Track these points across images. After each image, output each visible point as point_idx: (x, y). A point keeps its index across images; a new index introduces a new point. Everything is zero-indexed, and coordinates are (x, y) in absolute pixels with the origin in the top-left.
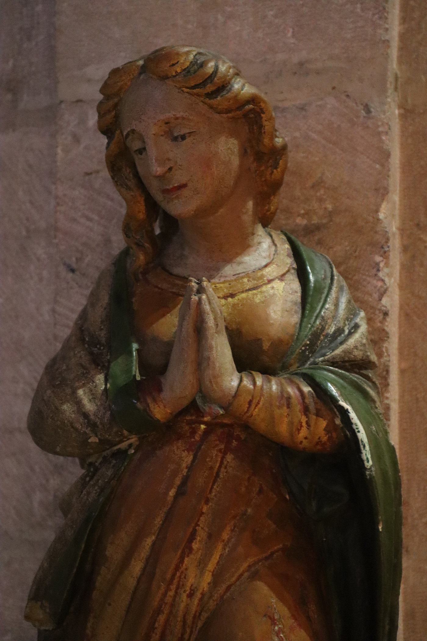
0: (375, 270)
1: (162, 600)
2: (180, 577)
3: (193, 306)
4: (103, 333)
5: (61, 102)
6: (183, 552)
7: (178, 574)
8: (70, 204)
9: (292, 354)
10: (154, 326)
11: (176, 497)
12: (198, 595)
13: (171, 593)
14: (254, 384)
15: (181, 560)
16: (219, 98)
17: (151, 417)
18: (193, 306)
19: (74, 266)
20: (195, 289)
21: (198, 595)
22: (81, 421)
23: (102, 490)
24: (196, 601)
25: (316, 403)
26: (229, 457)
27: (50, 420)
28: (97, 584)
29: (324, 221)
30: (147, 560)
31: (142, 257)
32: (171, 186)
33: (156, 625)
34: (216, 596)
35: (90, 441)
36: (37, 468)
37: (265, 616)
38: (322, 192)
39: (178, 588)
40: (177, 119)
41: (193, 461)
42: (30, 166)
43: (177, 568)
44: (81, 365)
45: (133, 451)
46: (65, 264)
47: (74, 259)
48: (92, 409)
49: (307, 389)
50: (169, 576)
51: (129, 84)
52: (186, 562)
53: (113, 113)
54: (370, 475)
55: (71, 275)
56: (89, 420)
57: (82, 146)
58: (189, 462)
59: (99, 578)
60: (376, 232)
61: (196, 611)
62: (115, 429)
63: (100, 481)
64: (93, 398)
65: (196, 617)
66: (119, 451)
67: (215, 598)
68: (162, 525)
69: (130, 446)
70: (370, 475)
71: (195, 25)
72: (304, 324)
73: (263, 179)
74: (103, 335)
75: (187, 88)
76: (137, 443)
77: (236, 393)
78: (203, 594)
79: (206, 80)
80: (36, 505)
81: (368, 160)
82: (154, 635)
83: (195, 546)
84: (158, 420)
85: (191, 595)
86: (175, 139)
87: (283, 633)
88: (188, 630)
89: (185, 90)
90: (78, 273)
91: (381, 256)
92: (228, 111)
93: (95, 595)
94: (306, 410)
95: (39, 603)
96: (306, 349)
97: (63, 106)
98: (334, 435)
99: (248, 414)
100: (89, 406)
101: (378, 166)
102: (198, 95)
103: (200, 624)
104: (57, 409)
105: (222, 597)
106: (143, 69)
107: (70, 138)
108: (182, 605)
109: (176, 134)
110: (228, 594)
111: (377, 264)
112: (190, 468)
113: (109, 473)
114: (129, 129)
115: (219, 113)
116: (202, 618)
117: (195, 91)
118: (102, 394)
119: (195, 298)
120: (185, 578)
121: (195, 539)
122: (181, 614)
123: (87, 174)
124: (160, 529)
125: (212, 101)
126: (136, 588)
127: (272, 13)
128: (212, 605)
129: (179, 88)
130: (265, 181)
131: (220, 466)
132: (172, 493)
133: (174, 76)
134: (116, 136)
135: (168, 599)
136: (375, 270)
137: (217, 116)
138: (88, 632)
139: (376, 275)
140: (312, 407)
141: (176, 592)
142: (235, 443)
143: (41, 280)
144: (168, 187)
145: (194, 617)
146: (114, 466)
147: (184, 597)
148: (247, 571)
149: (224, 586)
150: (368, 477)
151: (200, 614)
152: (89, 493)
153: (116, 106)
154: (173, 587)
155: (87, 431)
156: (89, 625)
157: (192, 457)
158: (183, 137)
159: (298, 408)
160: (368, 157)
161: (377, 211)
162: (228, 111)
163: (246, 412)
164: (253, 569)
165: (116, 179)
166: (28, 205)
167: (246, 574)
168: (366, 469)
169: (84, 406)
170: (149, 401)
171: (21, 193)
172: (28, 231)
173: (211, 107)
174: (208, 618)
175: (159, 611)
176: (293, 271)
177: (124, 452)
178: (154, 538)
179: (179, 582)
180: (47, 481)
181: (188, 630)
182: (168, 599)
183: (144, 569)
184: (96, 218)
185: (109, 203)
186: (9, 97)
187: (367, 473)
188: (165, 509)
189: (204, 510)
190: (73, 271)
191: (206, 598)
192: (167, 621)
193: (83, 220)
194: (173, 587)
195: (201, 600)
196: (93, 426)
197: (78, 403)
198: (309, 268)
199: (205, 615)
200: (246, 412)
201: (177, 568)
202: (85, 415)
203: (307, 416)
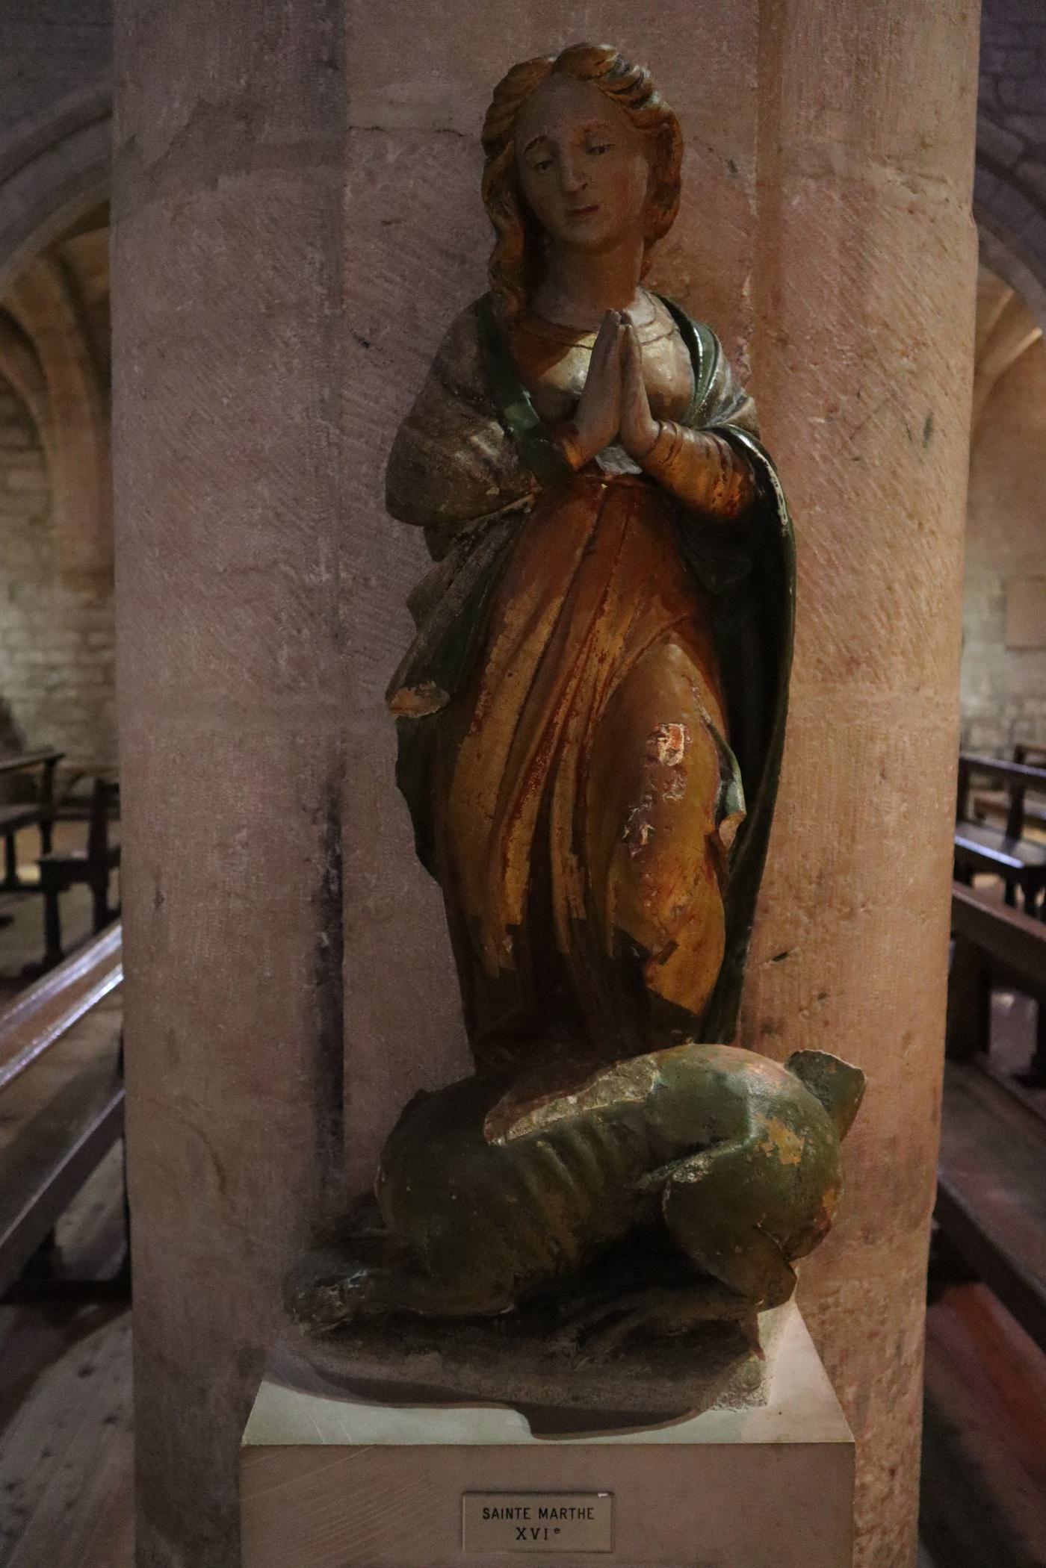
0: (737, 354)
1: (575, 663)
2: (592, 639)
3: (620, 335)
4: (479, 384)
5: (351, 128)
6: (595, 614)
7: (590, 636)
8: (363, 260)
9: (691, 414)
10: (547, 373)
11: (584, 556)
12: (609, 660)
13: (583, 656)
14: (675, 430)
15: (593, 623)
16: (642, 109)
17: (565, 460)
18: (620, 335)
19: (367, 339)
20: (619, 319)
21: (609, 660)
22: (481, 468)
23: (497, 552)
24: (606, 667)
25: (732, 457)
26: (633, 520)
27: (436, 472)
28: (493, 656)
29: (681, 295)
30: (556, 623)
31: (515, 302)
32: (584, 207)
33: (568, 690)
34: (629, 660)
35: (488, 493)
36: (284, 616)
37: (683, 676)
38: (679, 261)
39: (589, 652)
40: (599, 127)
41: (598, 520)
42: (274, 220)
43: (589, 631)
44: (463, 415)
45: (529, 510)
46: (355, 336)
47: (368, 331)
48: (494, 454)
49: (722, 442)
50: (583, 637)
51: (538, 82)
52: (597, 625)
53: (512, 118)
54: (786, 532)
55: (363, 350)
56: (491, 468)
57: (379, 186)
58: (594, 522)
59: (495, 649)
60: (739, 311)
61: (607, 678)
62: (522, 477)
63: (492, 544)
64: (494, 443)
65: (607, 683)
66: (511, 512)
67: (627, 663)
68: (571, 584)
69: (525, 505)
70: (786, 532)
71: (529, 45)
72: (699, 385)
73: (654, 221)
74: (479, 385)
75: (612, 91)
76: (533, 502)
77: (658, 437)
78: (614, 660)
79: (633, 85)
80: (282, 663)
81: (732, 226)
82: (565, 701)
83: (606, 607)
84: (571, 466)
85: (602, 660)
86: (591, 151)
87: (700, 694)
88: (598, 698)
89: (610, 94)
90: (372, 348)
91: (745, 338)
92: (646, 127)
93: (490, 668)
94: (723, 462)
95: (414, 689)
96: (704, 411)
97: (353, 133)
98: (746, 494)
99: (668, 462)
100: (490, 451)
101: (743, 234)
102: (621, 102)
103: (610, 692)
104: (447, 458)
105: (634, 662)
106: (556, 67)
107: (363, 175)
108: (594, 670)
109: (594, 145)
110: (641, 658)
111: (740, 347)
112: (596, 527)
113: (505, 533)
114: (537, 136)
115: (638, 127)
116: (613, 685)
117: (620, 97)
118: (504, 440)
119: (622, 327)
120: (597, 640)
121: (606, 600)
122: (591, 679)
123: (386, 223)
124: (569, 590)
125: (634, 111)
126: (544, 655)
127: (623, 40)
128: (624, 671)
129: (603, 92)
130: (655, 223)
131: (625, 528)
132: (579, 552)
133: (600, 77)
134: (508, 147)
135: (580, 663)
136: (737, 354)
137: (634, 130)
138: (479, 712)
139: (738, 360)
140: (729, 459)
141: (588, 657)
142: (636, 506)
143: (290, 371)
144: (578, 207)
145: (605, 685)
146: (508, 526)
147: (595, 661)
148: (660, 635)
149: (638, 650)
150: (784, 535)
151: (611, 681)
152: (478, 558)
153: (517, 109)
154: (585, 650)
155: (488, 480)
156: (480, 704)
157: (596, 516)
158: (602, 150)
159: (717, 459)
160: (732, 223)
161: (741, 287)
162: (646, 127)
163: (667, 459)
164: (665, 634)
165: (491, 205)
166: (271, 272)
167: (658, 639)
168: (782, 526)
169: (483, 452)
170: (565, 443)
171: (259, 257)
172: (268, 308)
173: (632, 119)
174: (620, 685)
175: (570, 675)
176: (676, 333)
177: (518, 513)
178: (562, 599)
179: (591, 644)
180: (299, 631)
181: (598, 698)
182: (580, 663)
183: (553, 634)
184: (398, 279)
185: (415, 260)
186: (241, 125)
187: (784, 530)
188: (573, 569)
189: (614, 571)
190: (366, 345)
191: (617, 663)
192: (578, 688)
193: (379, 281)
194: (585, 650)
195: (612, 665)
196: (497, 474)
197: (476, 450)
198: (695, 331)
199: (616, 682)
200: (667, 459)
201: (589, 631)
202: (487, 462)
203: (724, 468)
